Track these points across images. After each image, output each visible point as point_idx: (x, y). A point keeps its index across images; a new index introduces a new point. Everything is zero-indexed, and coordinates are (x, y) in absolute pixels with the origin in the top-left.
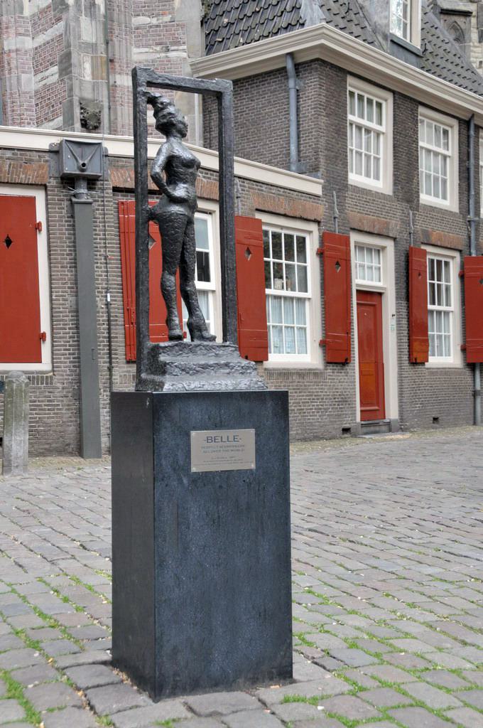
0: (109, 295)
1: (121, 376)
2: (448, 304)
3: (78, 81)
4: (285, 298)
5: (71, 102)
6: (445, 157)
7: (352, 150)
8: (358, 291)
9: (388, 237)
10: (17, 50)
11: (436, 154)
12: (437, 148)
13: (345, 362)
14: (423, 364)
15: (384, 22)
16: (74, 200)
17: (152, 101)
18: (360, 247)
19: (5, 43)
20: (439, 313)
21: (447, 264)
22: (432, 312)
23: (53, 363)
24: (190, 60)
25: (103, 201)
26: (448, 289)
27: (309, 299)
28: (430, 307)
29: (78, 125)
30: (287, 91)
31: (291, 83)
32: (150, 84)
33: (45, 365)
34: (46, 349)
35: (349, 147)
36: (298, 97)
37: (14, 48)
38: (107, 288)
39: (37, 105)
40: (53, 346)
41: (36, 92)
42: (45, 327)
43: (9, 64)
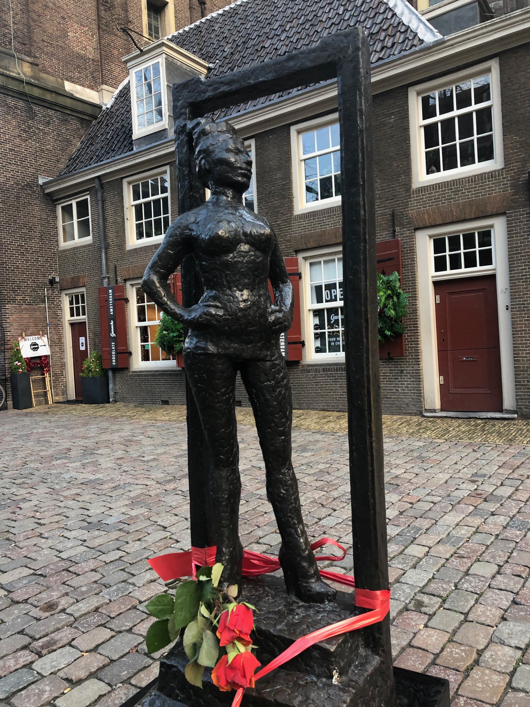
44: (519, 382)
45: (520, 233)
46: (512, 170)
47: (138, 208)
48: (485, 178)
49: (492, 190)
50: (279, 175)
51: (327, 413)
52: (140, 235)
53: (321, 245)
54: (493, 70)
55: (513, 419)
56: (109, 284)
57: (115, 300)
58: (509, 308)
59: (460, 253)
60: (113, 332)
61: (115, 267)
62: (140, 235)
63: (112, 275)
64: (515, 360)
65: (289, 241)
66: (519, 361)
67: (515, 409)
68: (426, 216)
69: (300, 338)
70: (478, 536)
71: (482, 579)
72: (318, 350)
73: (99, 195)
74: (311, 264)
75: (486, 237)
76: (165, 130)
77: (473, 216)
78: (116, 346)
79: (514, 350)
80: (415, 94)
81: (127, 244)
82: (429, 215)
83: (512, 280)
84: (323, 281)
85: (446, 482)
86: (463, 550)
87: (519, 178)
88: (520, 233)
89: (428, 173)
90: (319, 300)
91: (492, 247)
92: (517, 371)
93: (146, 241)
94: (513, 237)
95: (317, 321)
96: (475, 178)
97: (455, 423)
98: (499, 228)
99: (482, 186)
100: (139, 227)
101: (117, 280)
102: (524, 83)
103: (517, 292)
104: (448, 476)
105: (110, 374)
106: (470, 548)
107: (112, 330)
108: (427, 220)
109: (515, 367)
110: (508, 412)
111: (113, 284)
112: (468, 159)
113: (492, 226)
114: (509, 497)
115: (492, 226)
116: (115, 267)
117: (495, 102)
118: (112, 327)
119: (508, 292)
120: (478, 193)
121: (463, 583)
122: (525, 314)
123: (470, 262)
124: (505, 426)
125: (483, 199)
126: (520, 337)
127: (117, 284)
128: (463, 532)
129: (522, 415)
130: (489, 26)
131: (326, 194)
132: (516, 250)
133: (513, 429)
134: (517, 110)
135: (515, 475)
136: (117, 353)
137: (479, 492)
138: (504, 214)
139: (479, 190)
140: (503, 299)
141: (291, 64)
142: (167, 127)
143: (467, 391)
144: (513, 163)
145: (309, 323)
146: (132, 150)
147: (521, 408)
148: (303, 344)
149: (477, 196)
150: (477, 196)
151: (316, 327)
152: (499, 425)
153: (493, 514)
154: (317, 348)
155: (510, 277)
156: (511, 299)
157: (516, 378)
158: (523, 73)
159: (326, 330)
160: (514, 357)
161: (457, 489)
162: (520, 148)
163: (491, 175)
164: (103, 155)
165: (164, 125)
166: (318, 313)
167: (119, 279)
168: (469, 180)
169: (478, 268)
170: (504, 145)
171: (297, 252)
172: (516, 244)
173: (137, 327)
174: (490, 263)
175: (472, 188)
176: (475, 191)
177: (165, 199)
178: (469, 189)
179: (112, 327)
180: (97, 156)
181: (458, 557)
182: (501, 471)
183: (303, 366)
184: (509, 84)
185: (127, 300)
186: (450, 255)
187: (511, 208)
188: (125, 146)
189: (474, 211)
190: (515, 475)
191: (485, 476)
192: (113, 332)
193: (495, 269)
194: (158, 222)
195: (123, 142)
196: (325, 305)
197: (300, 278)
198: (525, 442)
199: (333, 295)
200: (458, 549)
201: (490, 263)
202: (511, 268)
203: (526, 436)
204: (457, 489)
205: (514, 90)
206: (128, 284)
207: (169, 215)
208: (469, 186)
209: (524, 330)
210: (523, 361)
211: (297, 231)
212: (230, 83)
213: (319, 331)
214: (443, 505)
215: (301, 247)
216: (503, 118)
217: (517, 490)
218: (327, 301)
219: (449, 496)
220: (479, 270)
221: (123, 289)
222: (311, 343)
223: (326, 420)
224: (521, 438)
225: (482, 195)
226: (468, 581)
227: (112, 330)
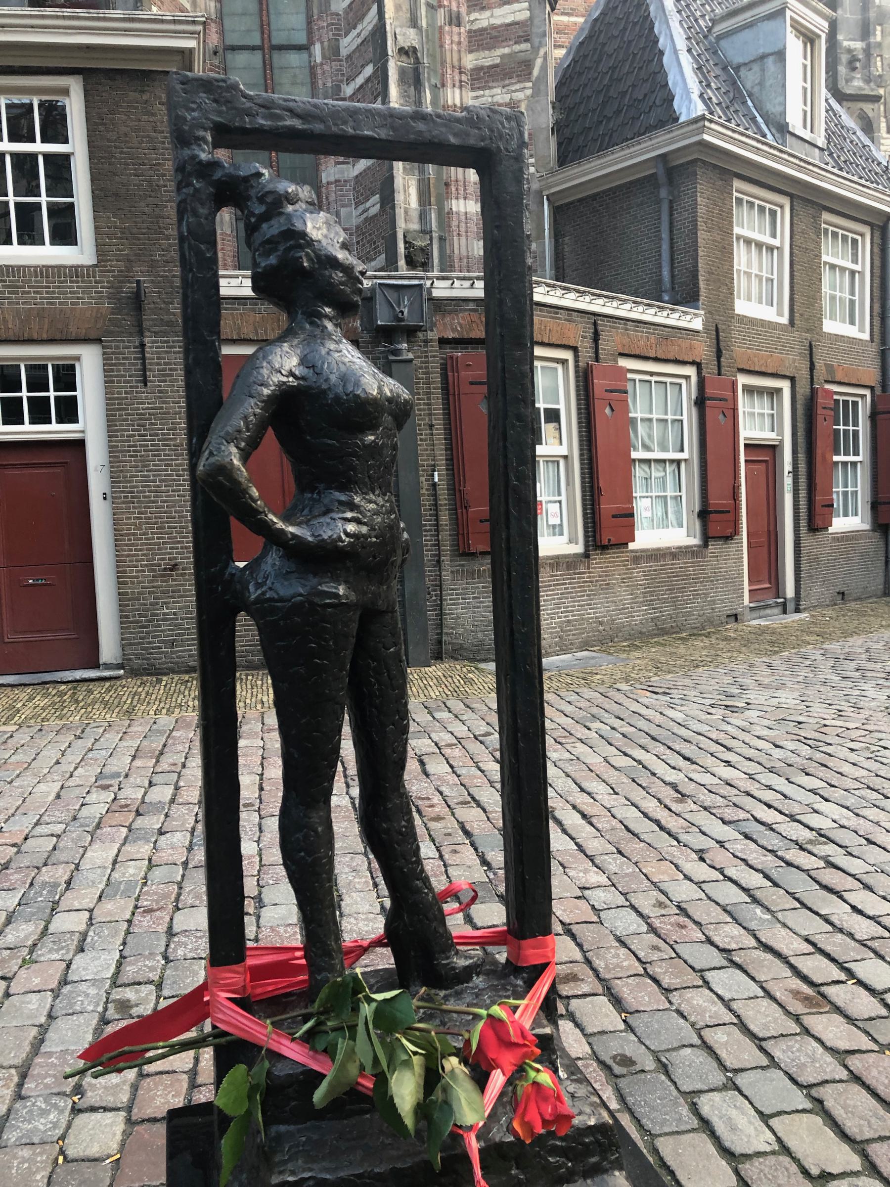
0: (436, 474)
1: (452, 572)
2: (856, 453)
3: (402, 210)
4: (657, 461)
5: (394, 236)
6: (853, 273)
7: (739, 271)
8: (746, 445)
9: (784, 377)
10: (337, 181)
11: (843, 269)
12: (845, 262)
13: (729, 536)
14: (826, 529)
15: (779, 109)
16: (391, 358)
17: (232, 191)
18: (750, 390)
19: (323, 175)
20: (845, 464)
21: (855, 404)
22: (837, 463)
24: (538, 175)
25: (426, 357)
26: (856, 433)
27: (686, 460)
28: (836, 458)
29: (402, 263)
30: (659, 202)
31: (663, 193)
32: (226, 135)
35: (736, 267)
36: (671, 208)
37: (332, 179)
38: (434, 466)
39: (358, 243)
41: (357, 227)
43: (327, 198)
44: (127, 617)
45: (125, 376)
46: (109, 271)
48: (65, 274)
49: (78, 298)
58: (109, 497)
59: (21, 398)
64: (119, 583)
66: (125, 583)
67: (120, 661)
70: (157, 873)
71: (199, 934)
75: (66, 376)
77: (45, 337)
79: (118, 567)
83: (114, 453)
85: (58, 796)
86: (147, 900)
87: (121, 287)
88: (125, 376)
91: (78, 393)
92: (123, 600)
94: (113, 382)
96: (47, 271)
97: (23, 695)
98: (89, 364)
99: (59, 287)
103: (122, 471)
104: (56, 787)
106: (156, 893)
109: (119, 594)
110: (108, 666)
112: (29, 234)
113: (78, 358)
114: (172, 801)
115: (78, 358)
117: (76, 146)
119: (106, 470)
120: (53, 298)
121: (175, 950)
122: (134, 508)
123: (40, 414)
124: (108, 691)
126: (127, 545)
128: (131, 871)
129: (132, 670)
130: (69, 18)
132: (119, 404)
133: (126, 696)
137: (123, 802)
138: (98, 341)
139: (54, 292)
140: (97, 482)
141: (421, 126)
143: (38, 637)
144: (110, 260)
147: (130, 659)
149: (52, 304)
150: (52, 304)
152: (98, 690)
153: (161, 833)
155: (110, 447)
156: (112, 482)
157: (121, 611)
160: (118, 578)
161: (83, 805)
162: (121, 238)
163: (76, 271)
168: (36, 271)
169: (54, 426)
170: (96, 228)
172: (119, 393)
174: (77, 421)
175: (42, 287)
176: (47, 293)
178: (38, 287)
181: (144, 911)
182: (138, 763)
184: (102, 128)
187: (110, 333)
189: (46, 327)
191: (118, 775)
193: (83, 432)
198: (152, 713)
200: (137, 899)
201: (75, 420)
202: (111, 434)
203: (149, 703)
204: (83, 805)
205: (109, 140)
208: (36, 282)
209: (134, 535)
210: (133, 583)
212: (304, 116)
214: (74, 835)
216: (92, 180)
219: (75, 818)
220: (54, 430)
224: (143, 708)
225: (60, 304)
226: (179, 944)
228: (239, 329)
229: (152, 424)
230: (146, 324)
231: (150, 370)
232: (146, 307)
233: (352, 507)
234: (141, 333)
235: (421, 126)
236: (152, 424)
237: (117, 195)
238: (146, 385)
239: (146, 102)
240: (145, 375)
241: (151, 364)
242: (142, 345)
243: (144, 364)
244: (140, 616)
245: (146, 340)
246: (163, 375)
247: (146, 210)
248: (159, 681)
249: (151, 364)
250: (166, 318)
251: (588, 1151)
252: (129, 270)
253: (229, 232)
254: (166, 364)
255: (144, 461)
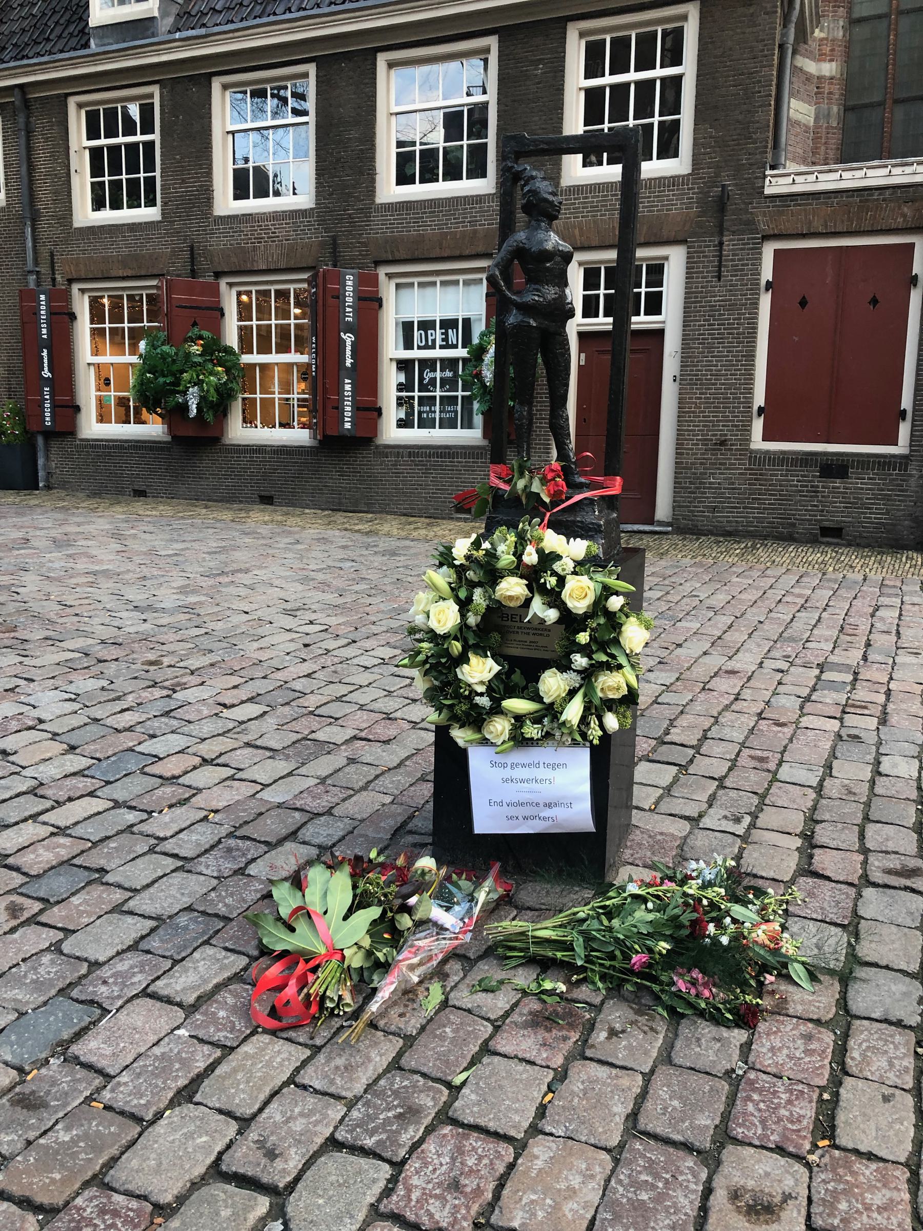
23: (911, 446)
33: (901, 448)
34: (904, 430)
40: (913, 426)
42: (907, 401)
44: (680, 483)
46: (700, 178)
47: (95, 153)
50: (354, 134)
51: (412, 519)
52: (98, 204)
53: (416, 256)
54: (690, 18)
55: (666, 533)
56: (38, 284)
57: (51, 313)
60: (46, 369)
61: (52, 255)
62: (98, 204)
63: (44, 269)
65: (365, 244)
66: (682, 454)
68: (577, 232)
69: (376, 402)
72: (403, 424)
73: (21, 119)
74: (398, 286)
76: (153, 19)
78: (53, 394)
80: (576, 34)
81: (74, 217)
82: (581, 229)
84: (416, 315)
89: (584, 166)
90: (408, 345)
91: (664, 289)
92: (679, 467)
93: (108, 216)
95: (402, 378)
100: (97, 188)
101: (54, 280)
102: (731, 49)
105: (40, 441)
107: (46, 365)
108: (578, 238)
110: (661, 523)
111: (47, 285)
113: (666, 258)
115: (666, 258)
116: (52, 255)
117: (688, 69)
118: (46, 360)
119: (679, 355)
125: (658, 216)
127: (54, 285)
129: (678, 528)
131: (427, 176)
133: (666, 545)
134: (716, 88)
135: (666, 582)
136: (54, 406)
140: (671, 365)
142: (156, 14)
145: (390, 379)
146: (86, 45)
148: (379, 411)
151: (400, 387)
154: (400, 420)
157: (676, 478)
158: (731, 33)
159: (416, 394)
164: (27, 45)
165: (152, 9)
166: (404, 365)
167: (59, 278)
171: (378, 263)
172: (697, 287)
173: (89, 364)
174: (660, 314)
177: (149, 146)
179: (46, 360)
180: (15, 45)
183: (377, 447)
185: (73, 317)
186: (605, 295)
188: (71, 34)
190: (666, 582)
192: (46, 369)
193: (664, 322)
194: (133, 185)
195: (67, 26)
196: (416, 354)
197: (381, 306)
199: (430, 338)
201: (660, 314)
202: (686, 324)
206: (75, 288)
207: (158, 174)
211: (378, 229)
213: (404, 394)
215: (384, 256)
217: (668, 593)
218: (419, 348)
221: (66, 296)
222: (392, 413)
223: (412, 527)
227: (46, 365)
228: (810, 223)
229: (720, 315)
230: (726, 224)
231: (725, 266)
232: (730, 207)
233: (538, 290)
234: (721, 234)
235: (593, 140)
236: (720, 315)
237: (716, 107)
238: (719, 280)
239: (752, 15)
240: (719, 271)
241: (727, 260)
242: (721, 244)
243: (720, 261)
244: (691, 483)
245: (725, 239)
246: (736, 271)
247: (740, 117)
248: (698, 539)
249: (727, 260)
250: (744, 217)
251: (590, 530)
252: (717, 175)
253: (835, 125)
254: (739, 260)
255: (710, 347)
